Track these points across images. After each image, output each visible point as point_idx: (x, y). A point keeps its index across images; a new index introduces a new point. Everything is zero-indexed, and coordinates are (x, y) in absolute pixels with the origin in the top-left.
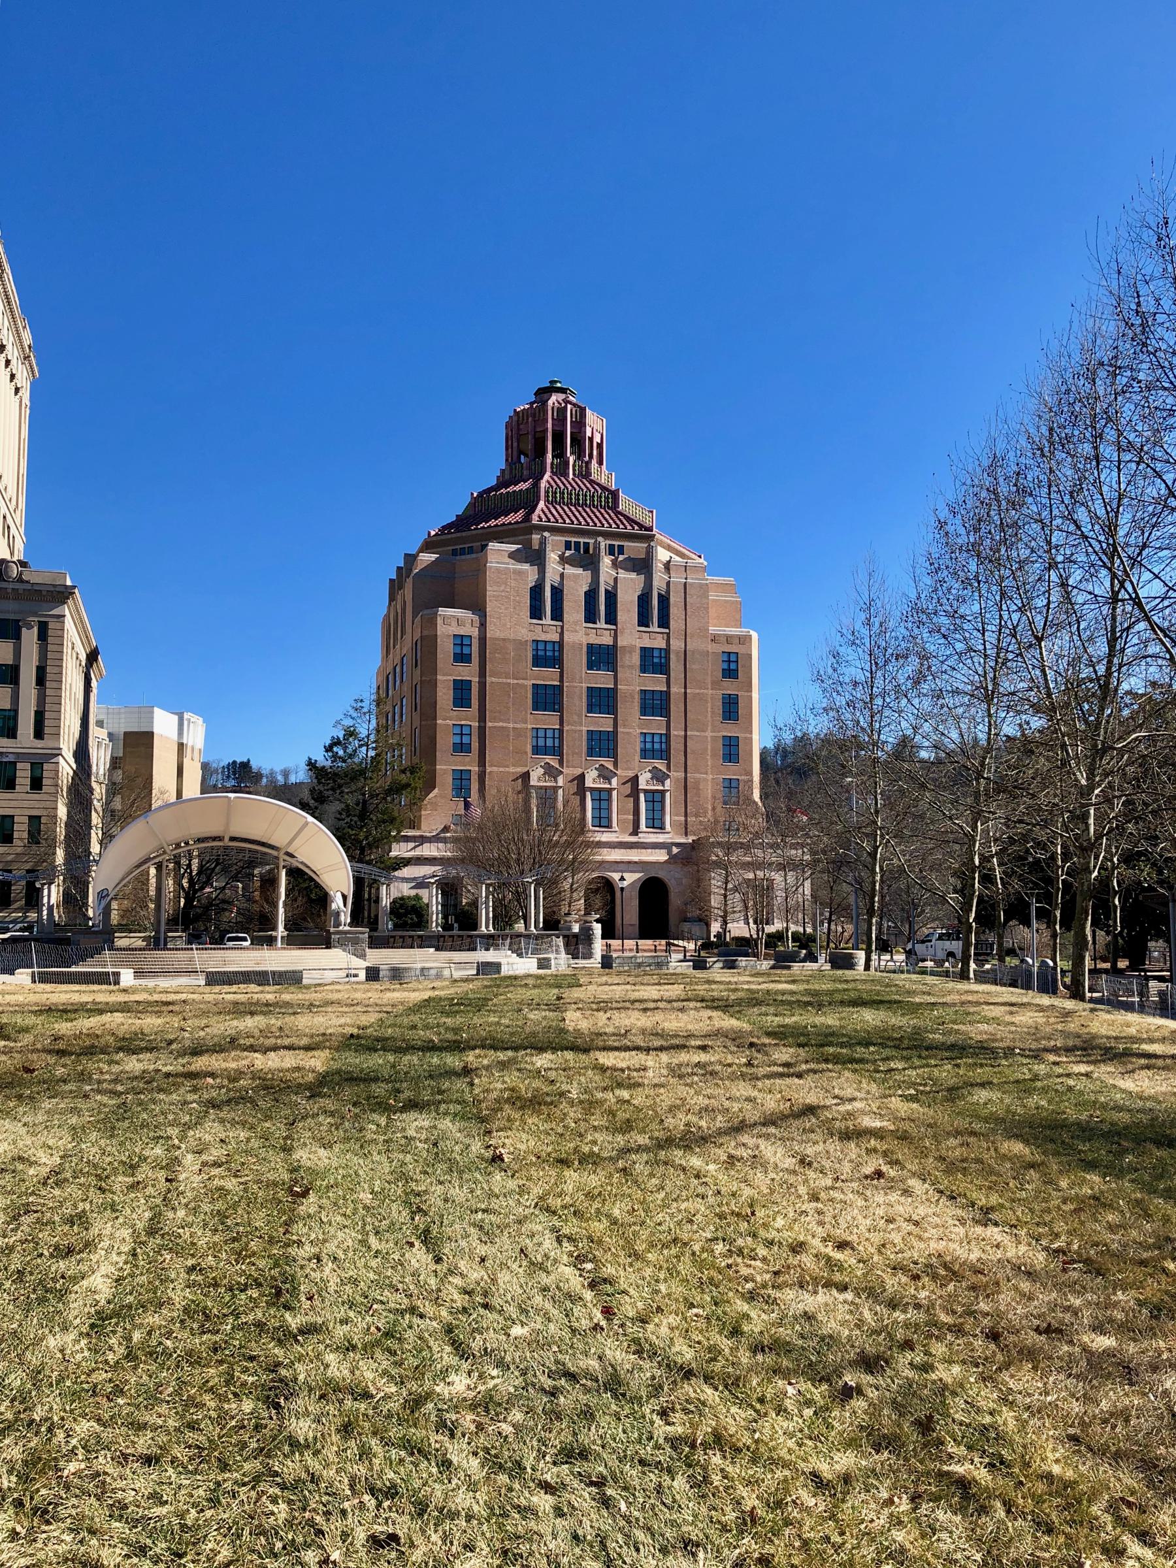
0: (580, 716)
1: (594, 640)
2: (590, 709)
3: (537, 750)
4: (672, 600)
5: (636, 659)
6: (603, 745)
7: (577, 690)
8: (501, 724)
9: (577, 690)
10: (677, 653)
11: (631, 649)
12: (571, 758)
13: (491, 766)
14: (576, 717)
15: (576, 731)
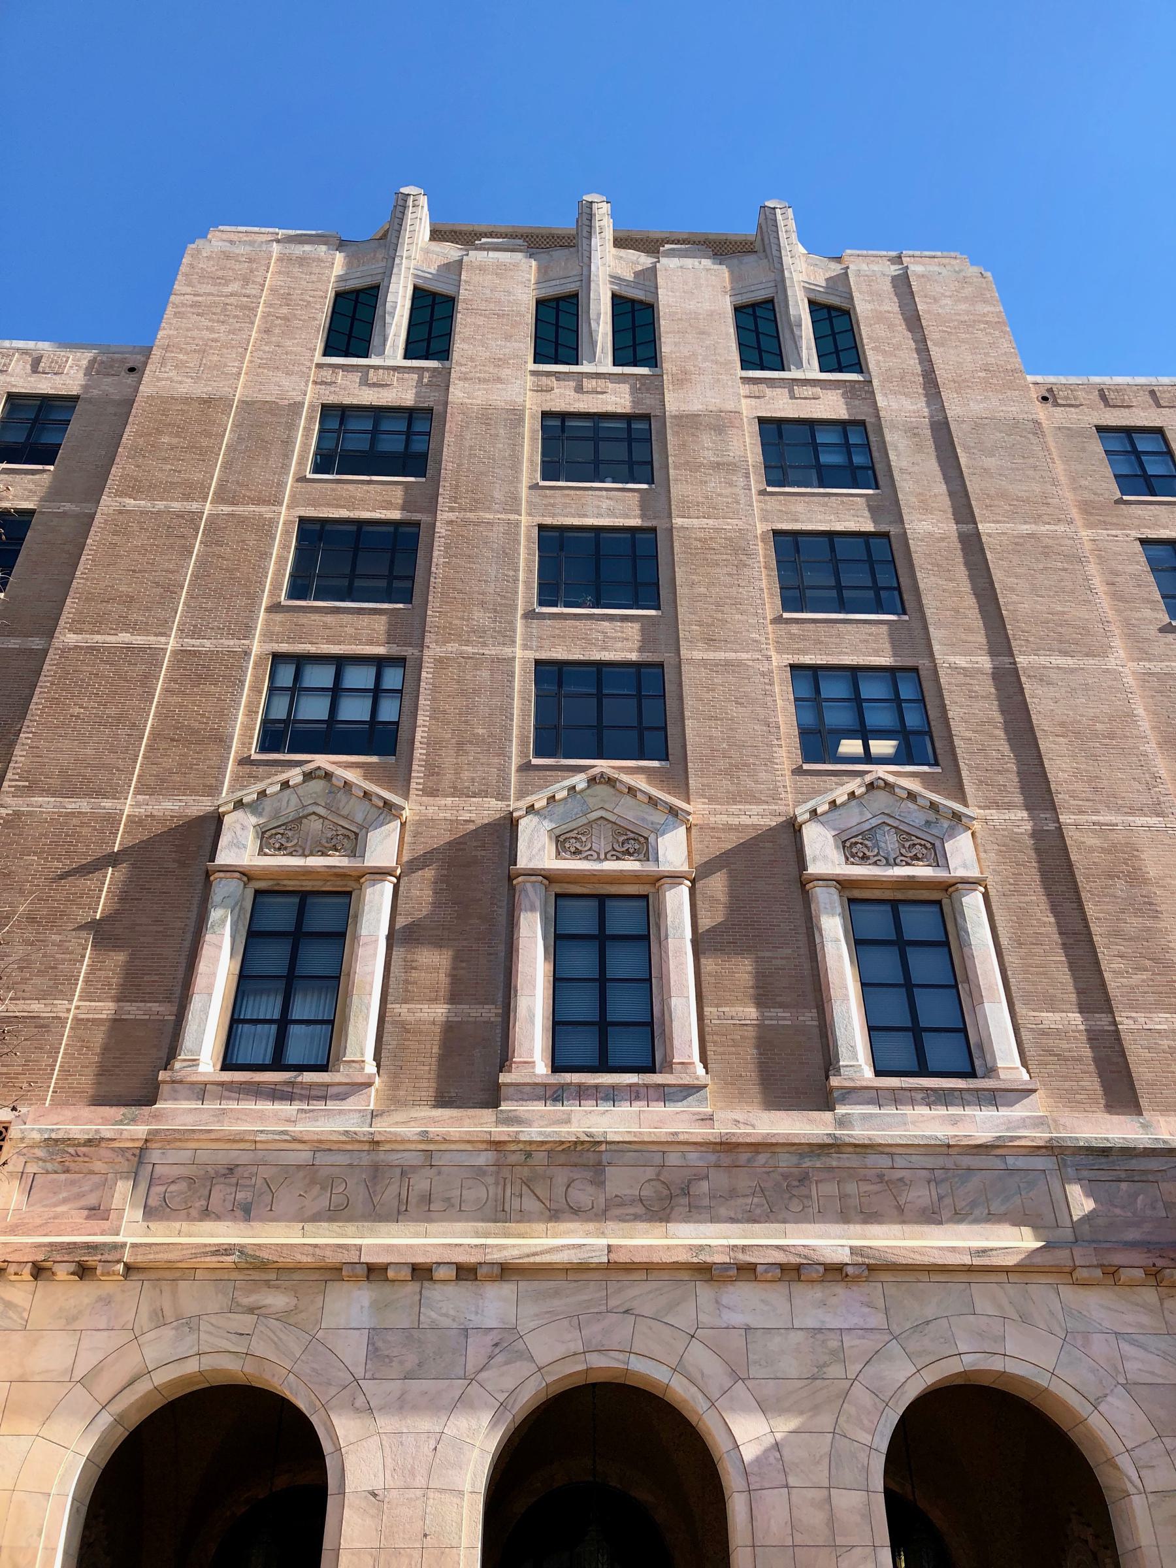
0: (502, 608)
1: (565, 399)
2: (550, 592)
3: (278, 736)
4: (863, 308)
5: (747, 447)
6: (607, 714)
7: (496, 535)
8: (125, 637)
9: (496, 535)
10: (912, 431)
11: (720, 423)
12: (448, 759)
13: (19, 792)
14: (480, 617)
15: (477, 661)
